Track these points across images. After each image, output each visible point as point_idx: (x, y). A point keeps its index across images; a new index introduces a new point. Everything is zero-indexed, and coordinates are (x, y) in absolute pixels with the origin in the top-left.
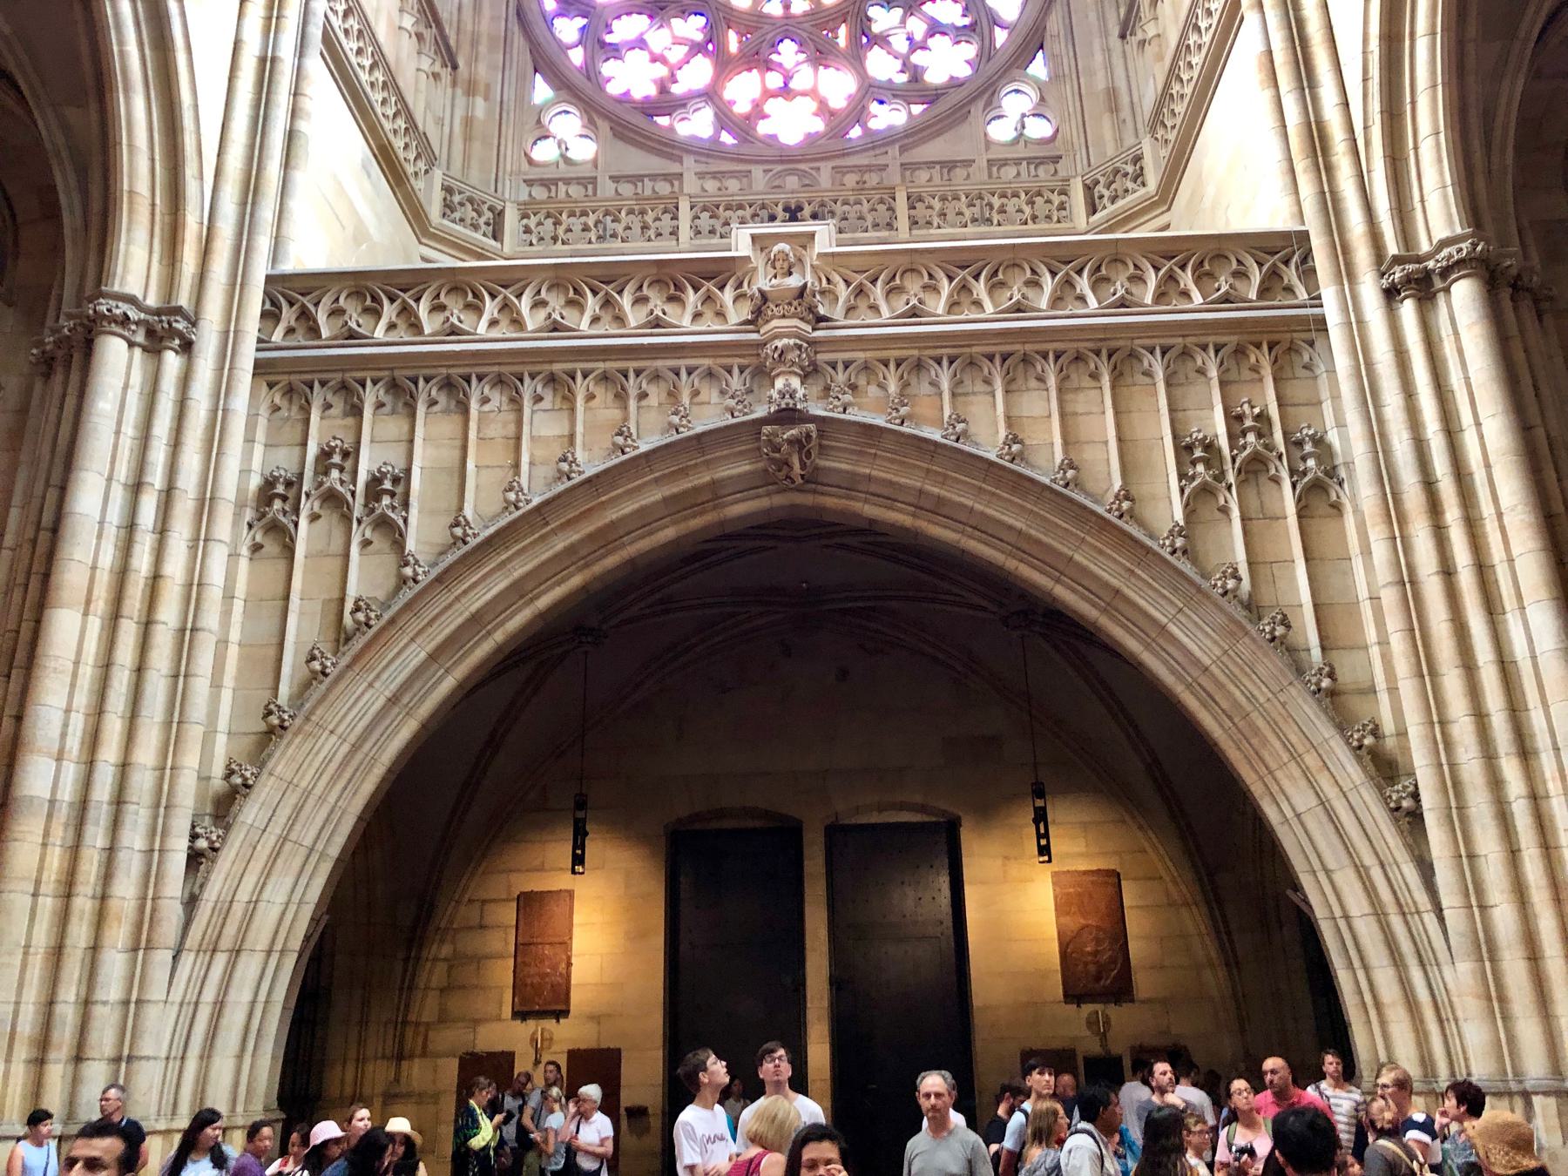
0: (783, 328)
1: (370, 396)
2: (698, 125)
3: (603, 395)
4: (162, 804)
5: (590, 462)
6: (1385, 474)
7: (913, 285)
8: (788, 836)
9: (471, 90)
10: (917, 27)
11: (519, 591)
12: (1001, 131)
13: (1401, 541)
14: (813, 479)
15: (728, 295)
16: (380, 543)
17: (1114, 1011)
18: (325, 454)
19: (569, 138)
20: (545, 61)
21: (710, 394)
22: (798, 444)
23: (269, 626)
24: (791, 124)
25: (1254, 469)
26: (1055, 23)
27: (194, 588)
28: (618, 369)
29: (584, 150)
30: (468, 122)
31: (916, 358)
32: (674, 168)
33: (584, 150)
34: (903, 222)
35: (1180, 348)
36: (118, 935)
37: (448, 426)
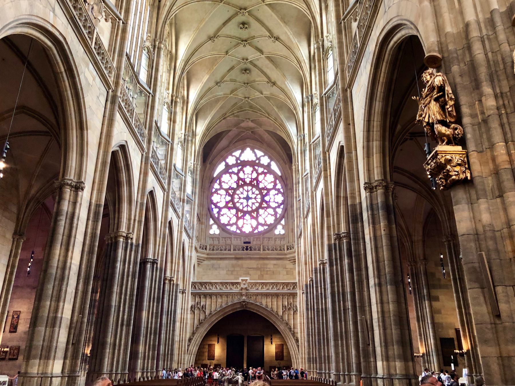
0: (244, 292)
1: (202, 296)
2: (233, 228)
3: (226, 297)
4: (185, 341)
5: (224, 306)
6: (300, 312)
7: (258, 285)
8: (242, 338)
9: (202, 224)
10: (266, 213)
11: (217, 319)
12: (277, 232)
13: (301, 319)
14: (246, 307)
15: (238, 286)
16: (203, 313)
17: (281, 362)
18: (197, 303)
19: (215, 230)
20: (212, 216)
21: (236, 297)
22: (245, 305)
23: (192, 322)
24: (247, 229)
25: (289, 309)
26: (286, 215)
27: (187, 318)
28: (227, 295)
29: (217, 232)
30: (202, 229)
31: (257, 295)
32: (230, 236)
33: (217, 232)
34: (262, 250)
35: (283, 295)
36: (183, 353)
37: (210, 300)
